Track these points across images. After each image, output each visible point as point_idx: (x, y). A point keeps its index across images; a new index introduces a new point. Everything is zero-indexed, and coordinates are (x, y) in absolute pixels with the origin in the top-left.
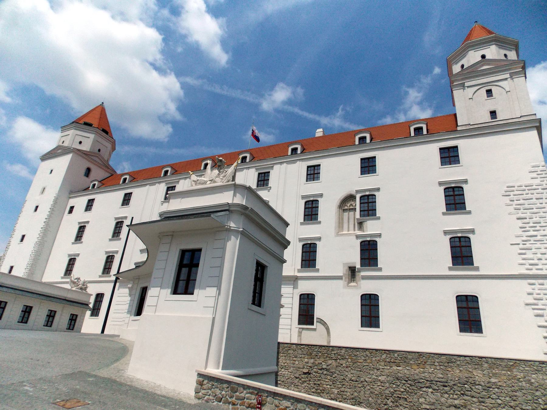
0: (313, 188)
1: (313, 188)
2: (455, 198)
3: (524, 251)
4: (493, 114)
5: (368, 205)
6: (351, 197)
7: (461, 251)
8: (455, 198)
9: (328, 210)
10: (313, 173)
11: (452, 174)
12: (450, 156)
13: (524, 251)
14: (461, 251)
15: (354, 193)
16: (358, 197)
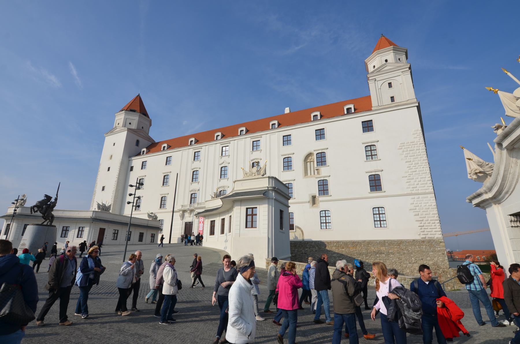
0: (287, 150)
1: (287, 150)
2: (371, 151)
3: (409, 181)
4: (392, 99)
5: (322, 159)
6: (310, 154)
7: (375, 183)
8: (371, 151)
9: (298, 163)
10: (287, 140)
11: (369, 137)
12: (368, 126)
13: (409, 181)
14: (375, 183)
15: (312, 151)
16: (315, 153)
